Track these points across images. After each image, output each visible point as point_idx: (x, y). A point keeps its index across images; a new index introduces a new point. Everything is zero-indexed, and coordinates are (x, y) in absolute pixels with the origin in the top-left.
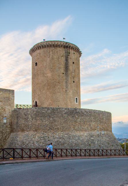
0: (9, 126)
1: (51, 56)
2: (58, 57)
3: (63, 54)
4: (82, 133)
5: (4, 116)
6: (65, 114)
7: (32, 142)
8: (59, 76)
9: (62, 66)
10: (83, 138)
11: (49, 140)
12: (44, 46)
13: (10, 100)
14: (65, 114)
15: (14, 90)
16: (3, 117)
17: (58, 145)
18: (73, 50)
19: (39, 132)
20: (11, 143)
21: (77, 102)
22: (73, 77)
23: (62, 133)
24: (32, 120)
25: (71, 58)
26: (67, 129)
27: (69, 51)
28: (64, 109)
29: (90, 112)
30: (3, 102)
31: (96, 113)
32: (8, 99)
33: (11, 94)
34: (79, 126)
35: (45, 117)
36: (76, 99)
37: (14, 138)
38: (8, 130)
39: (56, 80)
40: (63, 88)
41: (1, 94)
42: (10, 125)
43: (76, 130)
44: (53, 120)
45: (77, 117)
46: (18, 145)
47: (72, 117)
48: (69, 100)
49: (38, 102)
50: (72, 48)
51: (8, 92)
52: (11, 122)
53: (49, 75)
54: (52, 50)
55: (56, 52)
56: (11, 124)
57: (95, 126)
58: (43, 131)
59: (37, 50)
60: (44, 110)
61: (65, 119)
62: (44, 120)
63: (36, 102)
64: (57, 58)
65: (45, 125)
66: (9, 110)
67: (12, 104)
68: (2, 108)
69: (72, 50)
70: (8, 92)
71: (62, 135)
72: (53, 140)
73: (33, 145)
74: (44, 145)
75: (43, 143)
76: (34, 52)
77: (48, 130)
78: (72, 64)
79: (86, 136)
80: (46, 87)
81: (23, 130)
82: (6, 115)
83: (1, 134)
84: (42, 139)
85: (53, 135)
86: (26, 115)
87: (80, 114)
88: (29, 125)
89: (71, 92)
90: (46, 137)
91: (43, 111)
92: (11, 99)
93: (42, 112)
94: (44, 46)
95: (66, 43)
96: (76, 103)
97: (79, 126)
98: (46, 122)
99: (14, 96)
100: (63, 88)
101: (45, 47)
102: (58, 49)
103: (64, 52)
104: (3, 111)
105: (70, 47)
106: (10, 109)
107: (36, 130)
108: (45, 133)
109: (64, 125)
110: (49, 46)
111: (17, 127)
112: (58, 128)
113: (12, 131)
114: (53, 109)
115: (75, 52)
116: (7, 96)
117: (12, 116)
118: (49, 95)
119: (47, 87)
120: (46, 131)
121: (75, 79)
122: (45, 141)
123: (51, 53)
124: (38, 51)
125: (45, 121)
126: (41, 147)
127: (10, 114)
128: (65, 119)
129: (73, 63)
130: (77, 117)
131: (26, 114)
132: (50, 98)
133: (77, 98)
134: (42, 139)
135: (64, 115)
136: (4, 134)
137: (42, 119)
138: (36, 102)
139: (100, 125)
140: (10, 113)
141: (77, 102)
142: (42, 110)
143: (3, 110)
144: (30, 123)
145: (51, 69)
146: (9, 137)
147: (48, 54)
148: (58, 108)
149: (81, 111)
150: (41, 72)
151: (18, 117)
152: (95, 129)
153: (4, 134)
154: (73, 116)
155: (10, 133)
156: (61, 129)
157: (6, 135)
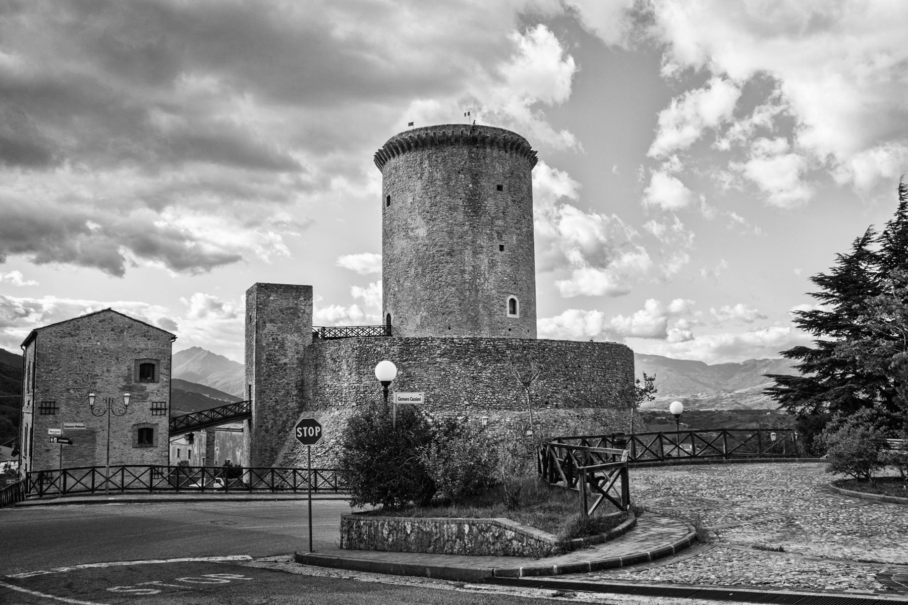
1: (426, 174)
2: (446, 176)
3: (463, 163)
4: (495, 417)
6: (441, 356)
10: (497, 431)
14: (441, 356)
15: (311, 287)
18: (499, 148)
21: (513, 312)
22: (498, 233)
26: (447, 403)
29: (524, 348)
31: (551, 350)
32: (294, 314)
33: (302, 299)
34: (487, 393)
36: (513, 302)
38: (292, 405)
40: (463, 272)
43: (476, 405)
45: (480, 365)
47: (465, 364)
48: (485, 308)
49: (392, 316)
50: (493, 142)
51: (294, 294)
52: (303, 381)
53: (422, 232)
54: (428, 157)
57: (547, 391)
59: (390, 158)
60: (381, 346)
63: (389, 315)
64: (444, 179)
66: (297, 344)
70: (294, 294)
79: (509, 426)
80: (413, 270)
82: (287, 361)
83: (272, 416)
86: (335, 362)
87: (490, 354)
92: (304, 313)
95: (474, 128)
96: (509, 315)
97: (487, 393)
99: (311, 305)
100: (463, 272)
101: (410, 149)
102: (448, 150)
105: (484, 139)
106: (300, 342)
109: (437, 391)
110: (420, 144)
111: (315, 394)
115: (506, 152)
116: (291, 305)
117: (301, 362)
118: (422, 293)
119: (416, 269)
121: (504, 237)
123: (426, 164)
130: (480, 365)
131: (335, 356)
132: (423, 303)
133: (515, 298)
135: (438, 360)
138: (389, 315)
139: (566, 388)
141: (513, 312)
144: (346, 385)
147: (419, 170)
148: (421, 339)
149: (494, 346)
150: (399, 226)
151: (316, 366)
152: (547, 403)
153: (281, 416)
154: (468, 364)
155: (300, 412)
157: (285, 418)
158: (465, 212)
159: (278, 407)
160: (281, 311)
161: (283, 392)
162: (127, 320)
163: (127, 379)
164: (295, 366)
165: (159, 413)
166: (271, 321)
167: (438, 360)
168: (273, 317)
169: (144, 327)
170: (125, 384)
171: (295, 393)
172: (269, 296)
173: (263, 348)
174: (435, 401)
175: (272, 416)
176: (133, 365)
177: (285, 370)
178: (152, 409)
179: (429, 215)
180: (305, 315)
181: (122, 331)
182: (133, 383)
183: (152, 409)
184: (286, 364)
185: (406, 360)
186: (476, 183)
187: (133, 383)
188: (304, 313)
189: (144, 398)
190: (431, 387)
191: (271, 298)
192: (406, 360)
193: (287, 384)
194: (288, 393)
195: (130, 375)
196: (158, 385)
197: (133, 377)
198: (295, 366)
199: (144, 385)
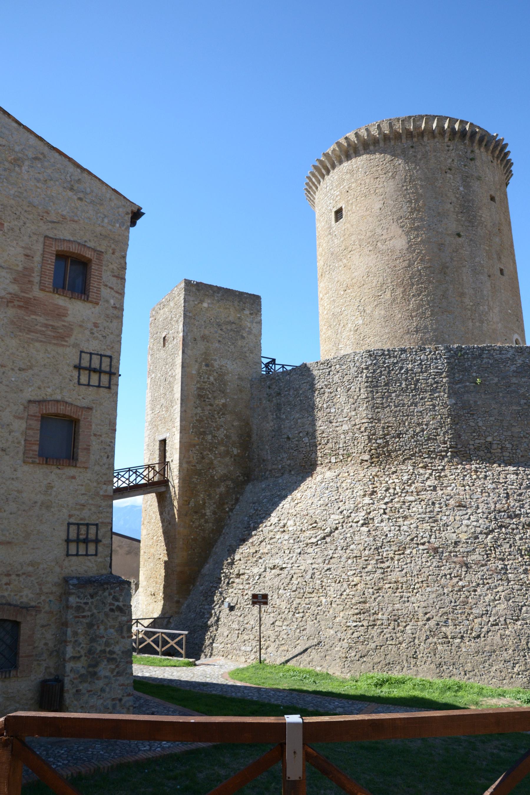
13: (243, 338)
14: (518, 373)
15: (253, 302)
18: (487, 151)
19: (393, 469)
25: (479, 178)
27: (472, 151)
28: (512, 352)
33: (247, 312)
41: (207, 309)
44: (463, 408)
61: (523, 402)
67: (252, 353)
69: (482, 149)
70: (236, 303)
76: (328, 172)
78: (486, 200)
80: (388, 293)
89: (496, 310)
93: (401, 368)
99: (260, 322)
103: (453, 154)
109: (516, 430)
116: (231, 319)
124: (346, 165)
128: (523, 402)
129: (492, 199)
134: (412, 498)
135: (514, 380)
144: (345, 427)
148: (483, 349)
151: (279, 407)
158: (458, 220)
160: (219, 325)
162: (33, 141)
163: (22, 277)
165: (95, 378)
167: (514, 380)
169: (71, 169)
170: (14, 288)
172: (202, 302)
176: (39, 247)
178: (78, 368)
180: (251, 337)
181: (17, 162)
182: (36, 292)
183: (78, 368)
185: (460, 381)
186: (467, 186)
187: (36, 292)
188: (250, 333)
189: (61, 337)
190: (505, 424)
191: (205, 305)
192: (460, 381)
195: (27, 272)
196: (97, 309)
197: (36, 279)
199: (61, 301)
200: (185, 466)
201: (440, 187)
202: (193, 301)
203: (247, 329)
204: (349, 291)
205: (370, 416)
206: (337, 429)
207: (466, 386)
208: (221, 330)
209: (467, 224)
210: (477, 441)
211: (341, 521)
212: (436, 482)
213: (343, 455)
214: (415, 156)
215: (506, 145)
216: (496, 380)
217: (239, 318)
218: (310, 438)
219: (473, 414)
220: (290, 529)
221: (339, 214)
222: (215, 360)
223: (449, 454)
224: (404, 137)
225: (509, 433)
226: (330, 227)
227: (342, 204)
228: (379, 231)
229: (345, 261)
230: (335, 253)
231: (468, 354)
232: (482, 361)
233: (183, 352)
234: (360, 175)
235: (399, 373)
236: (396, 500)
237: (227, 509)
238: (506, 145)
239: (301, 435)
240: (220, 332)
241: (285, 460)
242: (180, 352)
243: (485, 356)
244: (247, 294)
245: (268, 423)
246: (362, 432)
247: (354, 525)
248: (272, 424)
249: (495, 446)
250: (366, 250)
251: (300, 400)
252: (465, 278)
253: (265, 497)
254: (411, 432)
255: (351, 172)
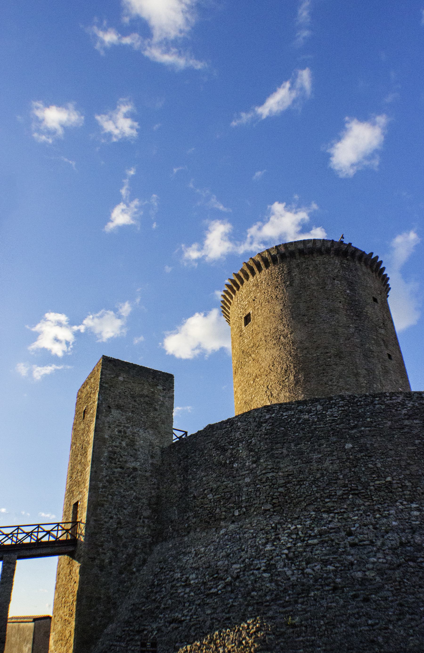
0: (147, 513)
3: (336, 271)
5: (127, 465)
6: (409, 417)
7: (262, 564)
8: (335, 334)
9: (341, 305)
11: (353, 545)
12: (270, 260)
13: (156, 410)
14: (409, 417)
16: (121, 468)
17: (411, 564)
19: (296, 516)
20: (153, 585)
23: (414, 505)
24: (254, 462)
28: (401, 397)
30: (126, 412)
33: (160, 387)
35: (319, 438)
37: (165, 561)
39: (326, 348)
42: (154, 511)
44: (360, 451)
46: (187, 585)
54: (298, 265)
55: (311, 269)
56: (157, 505)
58: (312, 507)
60: (309, 412)
61: (417, 442)
62: (316, 456)
64: (318, 284)
65: (323, 475)
67: (163, 423)
68: (120, 432)
69: (363, 264)
70: (150, 380)
71: (416, 513)
72: (379, 543)
73: (265, 575)
74: (335, 571)
75: (325, 563)
77: (342, 499)
78: (370, 301)
81: (211, 521)
82: (137, 465)
83: (111, 545)
84: (316, 541)
85: (370, 519)
86: (224, 450)
88: (241, 489)
90: (337, 530)
91: (306, 417)
93: (299, 419)
94: (270, 260)
98: (327, 463)
99: (172, 397)
104: (124, 444)
107: (277, 509)
108: (325, 515)
109: (414, 468)
112: (390, 482)
113: (159, 537)
114: (352, 401)
116: (145, 392)
117: (158, 471)
120: (329, 504)
122: (334, 553)
123: (295, 272)
125: (320, 461)
126: (316, 581)
127: (152, 464)
128: (417, 442)
134: (316, 541)
135: (406, 422)
136: (125, 546)
137: (302, 453)
140: (152, 457)
142: (301, 411)
143: (127, 440)
144: (247, 480)
145: (304, 316)
146: (144, 561)
151: (186, 469)
156: (404, 487)
157: (130, 551)
159: (121, 532)
160: (133, 397)
161: (130, 509)
164: (148, 474)
166: (118, 407)
167: (406, 422)
168: (121, 402)
171: (147, 513)
172: (118, 376)
173: (104, 441)
174: (415, 486)
175: (111, 545)
177: (134, 478)
179: (306, 318)
184: (135, 469)
188: (162, 405)
190: (403, 463)
191: (121, 378)
193: (136, 498)
194: (136, 514)
198: (148, 474)
200: (92, 523)
201: (330, 290)
202: (110, 374)
203: (160, 403)
204: (258, 380)
205: (269, 467)
206: (240, 482)
207: (361, 431)
208: (135, 401)
209: (355, 318)
210: (377, 482)
211: (242, 569)
212: (339, 524)
213: (245, 507)
214: (308, 268)
215: (381, 262)
216: (390, 423)
217: (153, 392)
218: (214, 494)
219: (371, 456)
220: (192, 582)
221: (247, 319)
222: (128, 428)
223: (351, 496)
224: (297, 255)
225: (408, 472)
226: (241, 331)
227: (250, 311)
228: (281, 327)
229: (253, 356)
230: (245, 350)
231: (360, 401)
232: (374, 407)
233: (97, 418)
234: (264, 286)
235: (297, 423)
236: (299, 544)
237: (134, 570)
238: (381, 262)
239: (206, 492)
240: (133, 403)
241: (191, 518)
242: (94, 419)
243: (376, 402)
244: (161, 372)
245: (176, 485)
246: (263, 483)
247: (256, 572)
248: (179, 485)
249: (395, 486)
250: (271, 344)
251: (205, 459)
252: (357, 360)
253: (171, 555)
254: (311, 478)
255: (257, 285)
